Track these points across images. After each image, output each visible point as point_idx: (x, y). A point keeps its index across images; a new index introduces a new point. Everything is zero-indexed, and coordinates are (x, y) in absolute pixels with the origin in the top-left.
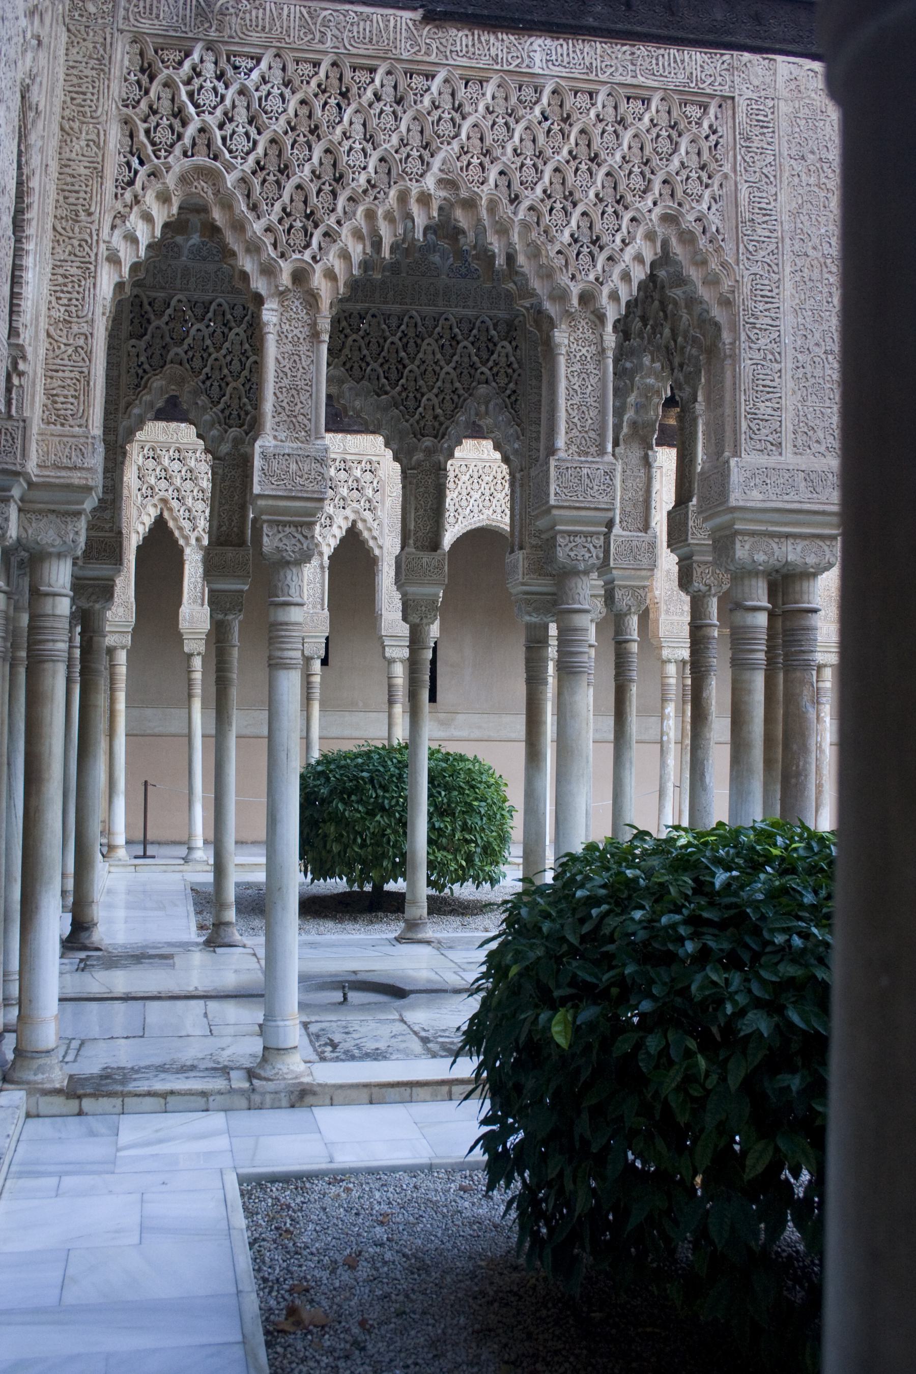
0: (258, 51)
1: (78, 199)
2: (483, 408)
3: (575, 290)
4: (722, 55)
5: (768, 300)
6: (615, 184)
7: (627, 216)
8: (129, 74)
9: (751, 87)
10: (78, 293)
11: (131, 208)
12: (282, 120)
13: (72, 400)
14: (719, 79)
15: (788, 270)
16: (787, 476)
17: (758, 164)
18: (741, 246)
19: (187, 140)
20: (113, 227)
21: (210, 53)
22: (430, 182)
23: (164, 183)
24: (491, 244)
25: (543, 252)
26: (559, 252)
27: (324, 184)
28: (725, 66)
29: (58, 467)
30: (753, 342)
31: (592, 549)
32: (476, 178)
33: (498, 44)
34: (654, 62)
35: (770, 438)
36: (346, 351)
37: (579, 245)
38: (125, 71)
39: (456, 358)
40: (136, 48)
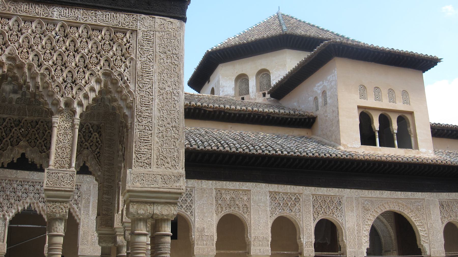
2: (86, 158)
4: (133, 15)
5: (147, 106)
14: (131, 23)
18: (137, 85)
25: (50, 86)
26: (57, 86)
28: (134, 19)
30: (140, 122)
31: (63, 208)
32: (24, 57)
34: (104, 16)
35: (146, 161)
36: (29, 135)
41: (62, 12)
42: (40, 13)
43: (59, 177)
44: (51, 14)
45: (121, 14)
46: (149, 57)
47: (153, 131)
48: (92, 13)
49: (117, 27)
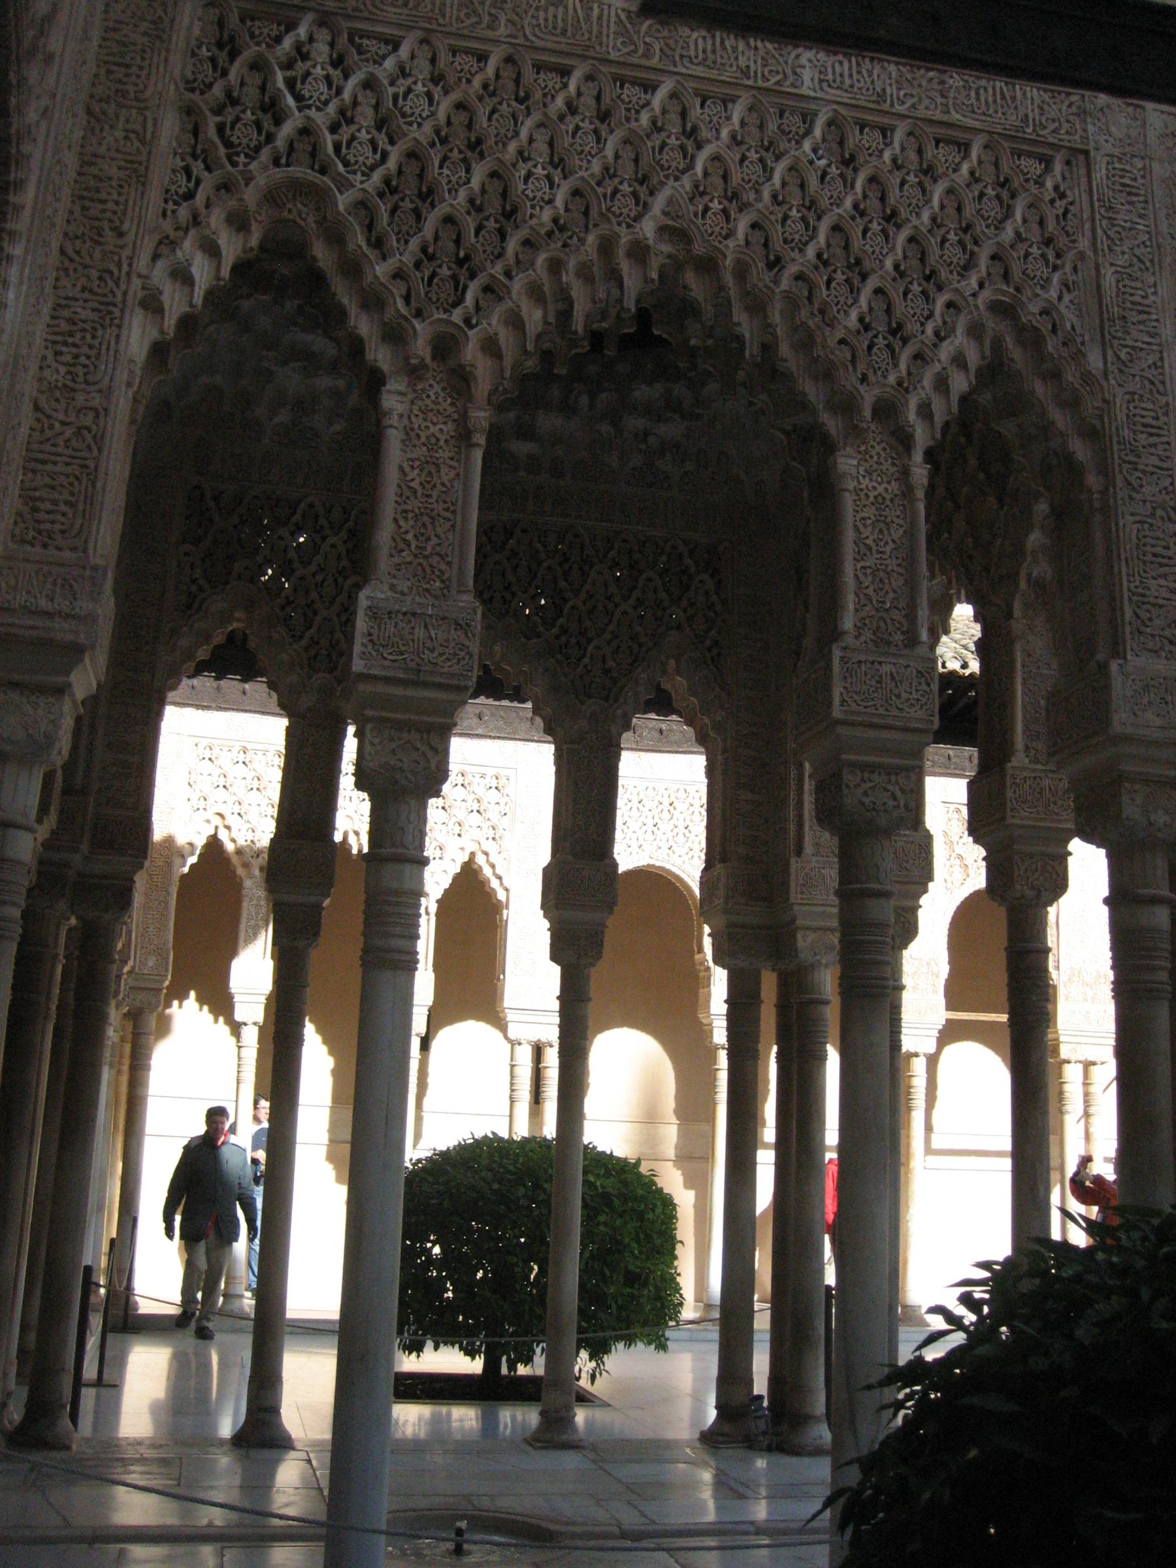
0: (396, 32)
1: (104, 211)
3: (868, 397)
4: (1068, 94)
6: (923, 253)
7: (941, 300)
8: (199, 47)
10: (91, 347)
11: (187, 230)
12: (428, 127)
13: (63, 508)
14: (1066, 126)
18: (1110, 352)
19: (280, 142)
20: (156, 257)
21: (325, 31)
22: (648, 228)
23: (241, 200)
24: (739, 324)
26: (842, 342)
27: (487, 219)
28: (1074, 109)
29: (31, 612)
30: (1134, 489)
31: (899, 794)
32: (717, 229)
34: (973, 93)
35: (1167, 633)
37: (871, 334)
38: (193, 42)
39: (637, 593)
40: (214, 14)
41: (830, 70)
42: (756, 72)
43: (881, 676)
44: (791, 79)
45: (1028, 89)
46: (1137, 252)
49: (1020, 135)
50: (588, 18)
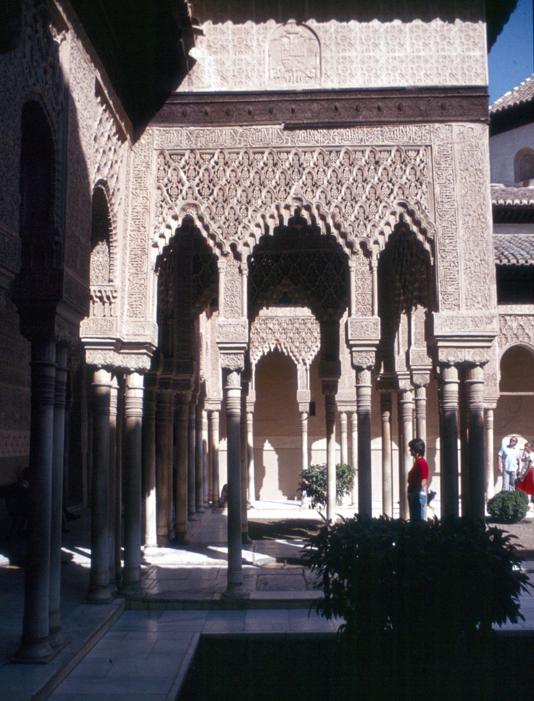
4: (425, 126)
9: (440, 140)
11: (162, 223)
15: (461, 223)
16: (463, 320)
17: (444, 175)
18: (437, 214)
19: (184, 193)
25: (342, 226)
26: (350, 225)
28: (427, 131)
29: (135, 335)
30: (444, 258)
31: (370, 358)
33: (319, 135)
34: (392, 133)
35: (454, 303)
41: (344, 135)
46: (448, 177)
47: (459, 267)
48: (378, 131)
50: (268, 134)
